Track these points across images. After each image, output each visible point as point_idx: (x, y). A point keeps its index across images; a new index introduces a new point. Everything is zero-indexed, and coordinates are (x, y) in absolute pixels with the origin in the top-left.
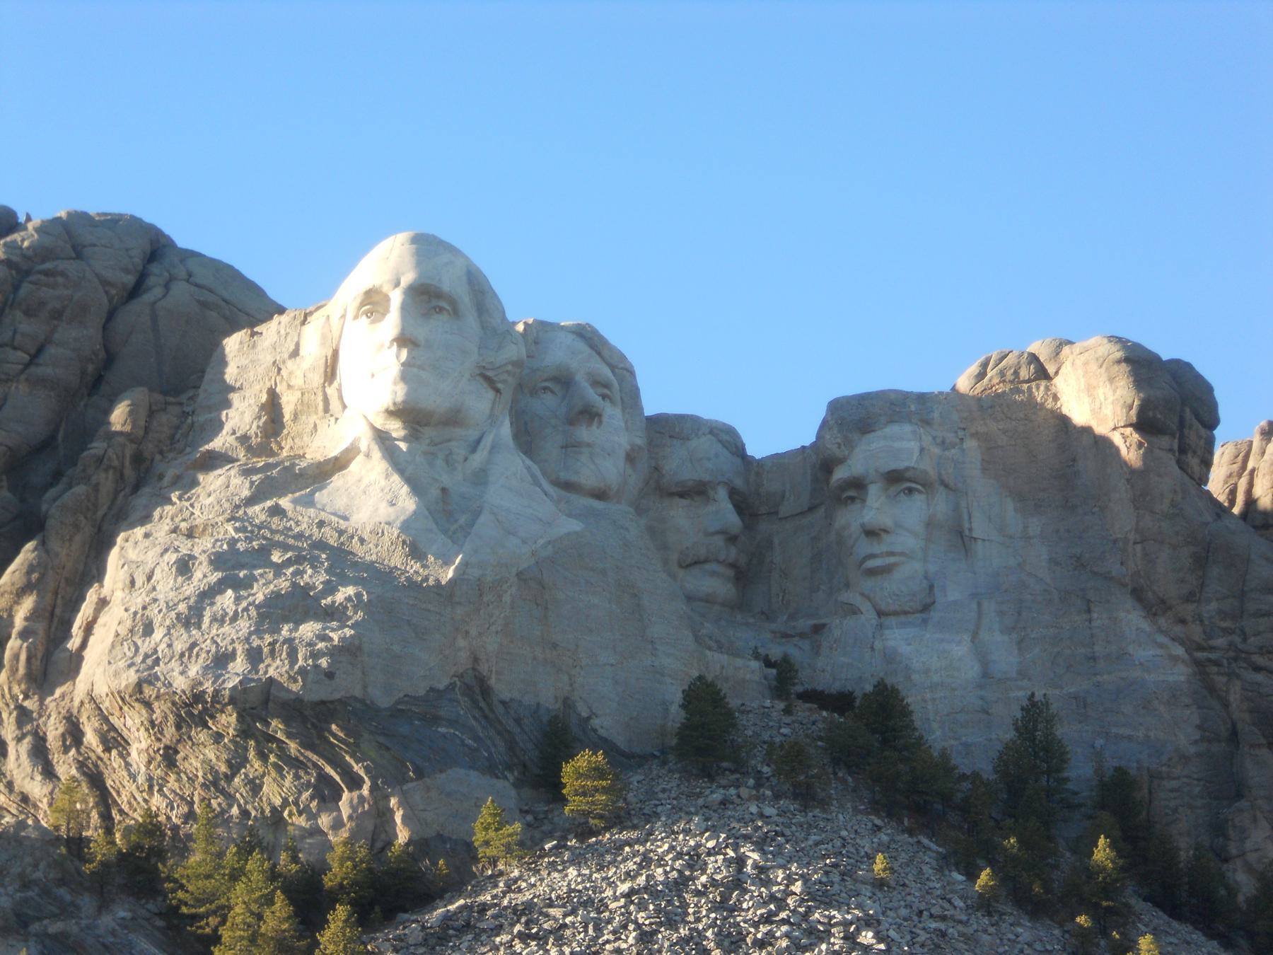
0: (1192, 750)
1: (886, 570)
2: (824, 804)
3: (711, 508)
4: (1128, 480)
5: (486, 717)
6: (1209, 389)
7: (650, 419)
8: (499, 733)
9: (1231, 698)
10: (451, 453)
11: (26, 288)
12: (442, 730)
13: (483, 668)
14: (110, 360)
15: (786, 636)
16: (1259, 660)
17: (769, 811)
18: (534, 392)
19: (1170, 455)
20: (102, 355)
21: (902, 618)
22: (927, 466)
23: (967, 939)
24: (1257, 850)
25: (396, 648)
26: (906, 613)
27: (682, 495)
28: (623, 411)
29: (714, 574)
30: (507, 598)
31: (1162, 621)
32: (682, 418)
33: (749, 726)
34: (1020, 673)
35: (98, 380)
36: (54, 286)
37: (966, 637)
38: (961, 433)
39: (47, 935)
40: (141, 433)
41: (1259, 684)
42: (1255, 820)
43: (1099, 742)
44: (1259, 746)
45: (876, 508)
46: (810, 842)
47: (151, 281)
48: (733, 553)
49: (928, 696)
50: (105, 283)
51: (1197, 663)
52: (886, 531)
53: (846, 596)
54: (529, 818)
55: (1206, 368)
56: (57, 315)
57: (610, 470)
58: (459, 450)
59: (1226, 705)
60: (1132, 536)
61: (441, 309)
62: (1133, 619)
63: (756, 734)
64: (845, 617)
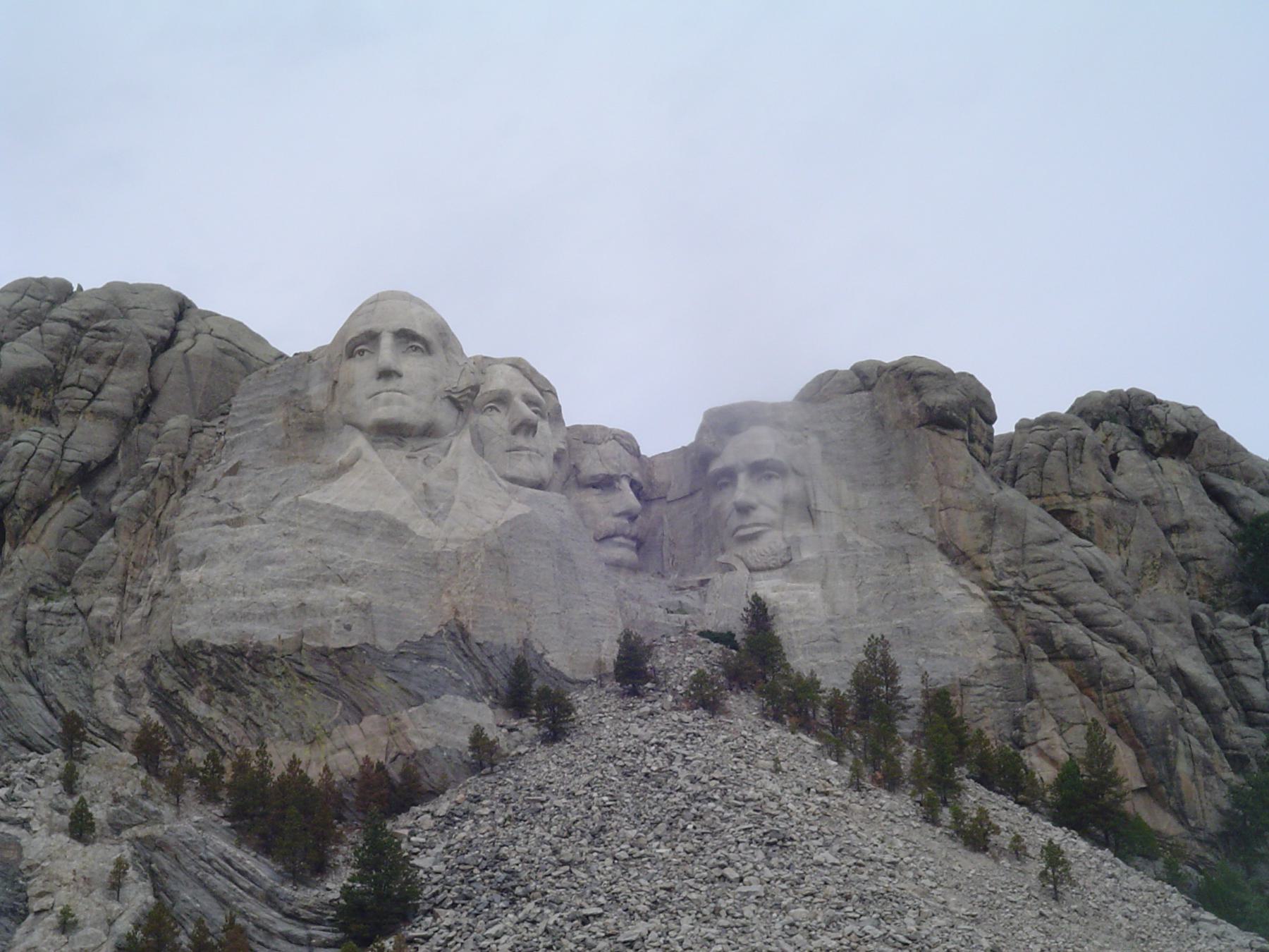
0: (992, 664)
1: (753, 537)
2: (727, 713)
4: (933, 464)
5: (466, 656)
6: (988, 394)
8: (477, 668)
9: (1018, 625)
10: (428, 457)
11: (85, 341)
12: (435, 667)
13: (463, 619)
14: (154, 394)
15: (681, 589)
16: (1040, 596)
17: (686, 718)
18: (483, 412)
19: (962, 444)
20: (149, 391)
21: (768, 573)
22: (780, 457)
23: (845, 808)
25: (397, 605)
26: (770, 569)
28: (550, 422)
29: (621, 545)
30: (478, 565)
31: (962, 568)
32: (592, 428)
33: (662, 659)
34: (860, 610)
36: (108, 340)
37: (818, 586)
39: (138, 839)
40: (186, 449)
42: (1043, 716)
43: (921, 661)
44: (1043, 660)
45: (744, 490)
47: (181, 334)
48: (634, 529)
49: (792, 630)
50: (149, 337)
51: (992, 598)
54: (504, 730)
55: (986, 380)
56: (112, 362)
57: (544, 468)
60: (938, 506)
61: (417, 348)
62: (940, 567)
63: (667, 662)
64: (724, 572)
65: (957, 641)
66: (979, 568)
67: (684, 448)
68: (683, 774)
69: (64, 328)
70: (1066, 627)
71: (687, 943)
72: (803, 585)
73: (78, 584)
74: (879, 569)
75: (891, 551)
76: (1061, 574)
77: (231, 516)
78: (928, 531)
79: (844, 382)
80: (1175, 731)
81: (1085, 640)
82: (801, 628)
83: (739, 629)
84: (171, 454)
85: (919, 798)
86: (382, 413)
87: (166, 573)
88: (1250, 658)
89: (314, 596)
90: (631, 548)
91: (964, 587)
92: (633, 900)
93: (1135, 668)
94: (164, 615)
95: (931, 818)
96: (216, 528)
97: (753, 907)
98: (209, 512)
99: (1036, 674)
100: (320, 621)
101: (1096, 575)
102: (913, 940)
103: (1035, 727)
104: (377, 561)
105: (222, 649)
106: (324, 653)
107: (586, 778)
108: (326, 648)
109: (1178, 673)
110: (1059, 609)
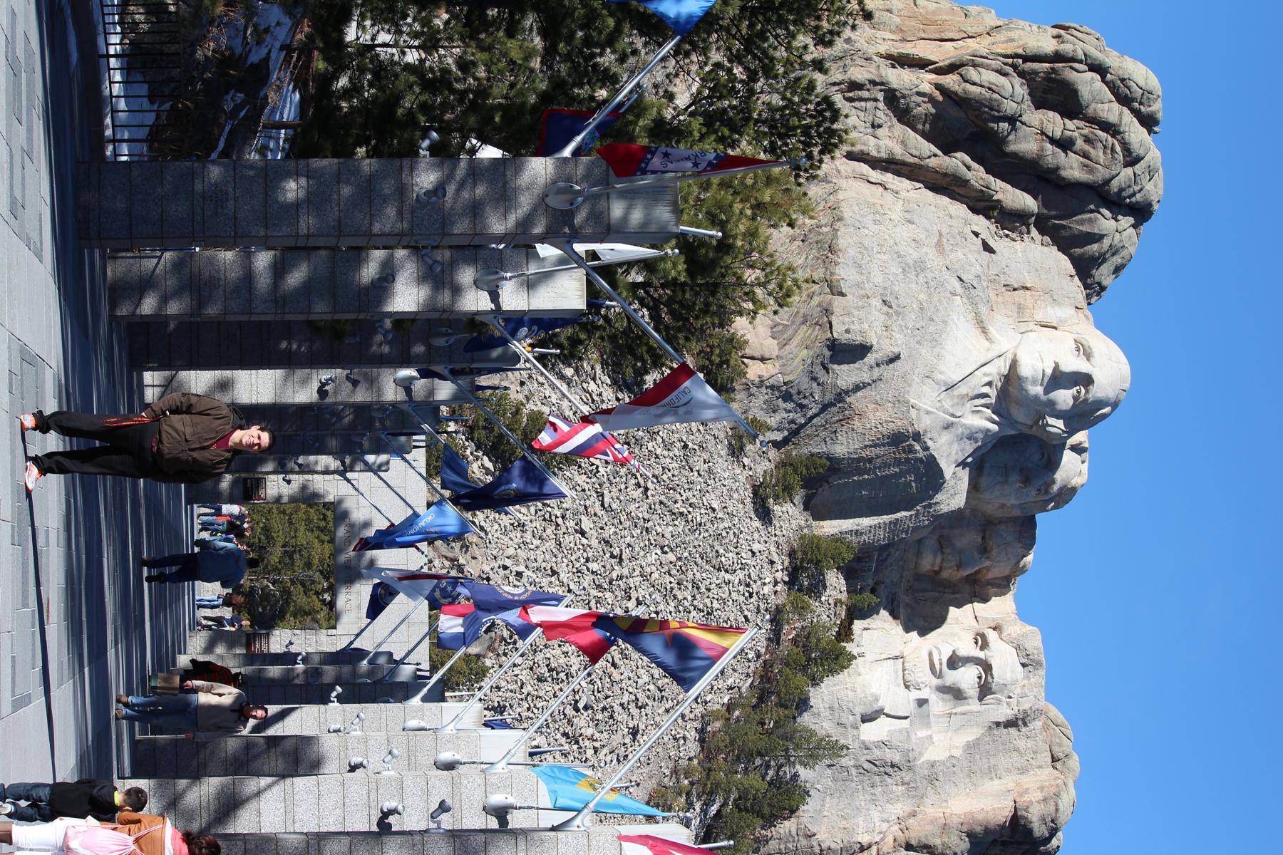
0: (815, 844)
3: (976, 555)
7: (1033, 517)
17: (766, 590)
27: (983, 538)
29: (935, 557)
34: (863, 742)
36: (1104, 153)
38: (1016, 709)
46: (746, 613)
69: (1113, 118)
71: (577, 565)
73: (900, 129)
74: (897, 758)
79: (1060, 745)
82: (850, 693)
90: (933, 565)
92: (613, 529)
105: (835, 236)
106: (827, 312)
107: (715, 505)
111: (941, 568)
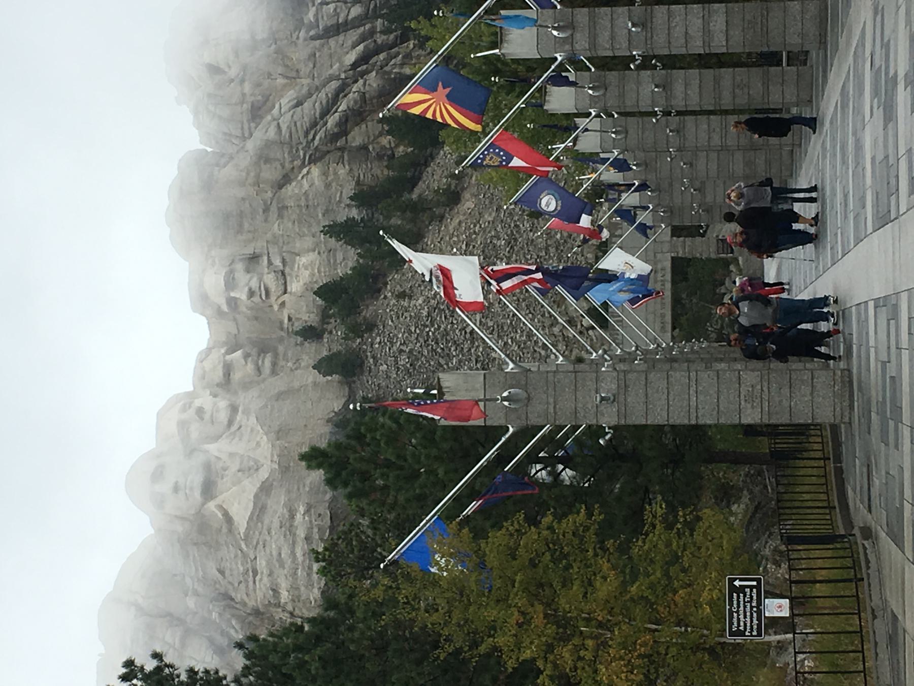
0: (347, 167)
9: (325, 148)
14: (169, 614)
16: (310, 137)
17: (378, 340)
24: (390, 143)
25: (307, 489)
26: (286, 283)
29: (263, 362)
35: (179, 619)
41: (321, 138)
42: (378, 143)
43: (343, 205)
48: (254, 352)
51: (309, 163)
52: (250, 289)
53: (276, 307)
57: (223, 404)
58: (221, 464)
59: (328, 152)
60: (256, 188)
62: (291, 189)
65: (334, 184)
66: (293, 168)
67: (208, 323)
68: (411, 346)
70: (329, 125)
72: (296, 266)
74: (290, 225)
75: (280, 216)
76: (298, 124)
77: (251, 574)
78: (270, 194)
80: (390, 73)
81: (337, 114)
83: (319, 301)
84: (211, 607)
85: (427, 223)
86: (197, 494)
87: (280, 610)
88: (335, 10)
89: (301, 533)
91: (303, 178)
93: (354, 90)
94: (304, 611)
95: (442, 218)
96: (257, 583)
97: (488, 320)
98: (247, 587)
99: (353, 145)
100: (316, 530)
101: (299, 104)
102: (510, 243)
103: (383, 148)
104: (283, 499)
108: (330, 527)
109: (354, 66)
110: (318, 127)
111: (259, 355)
